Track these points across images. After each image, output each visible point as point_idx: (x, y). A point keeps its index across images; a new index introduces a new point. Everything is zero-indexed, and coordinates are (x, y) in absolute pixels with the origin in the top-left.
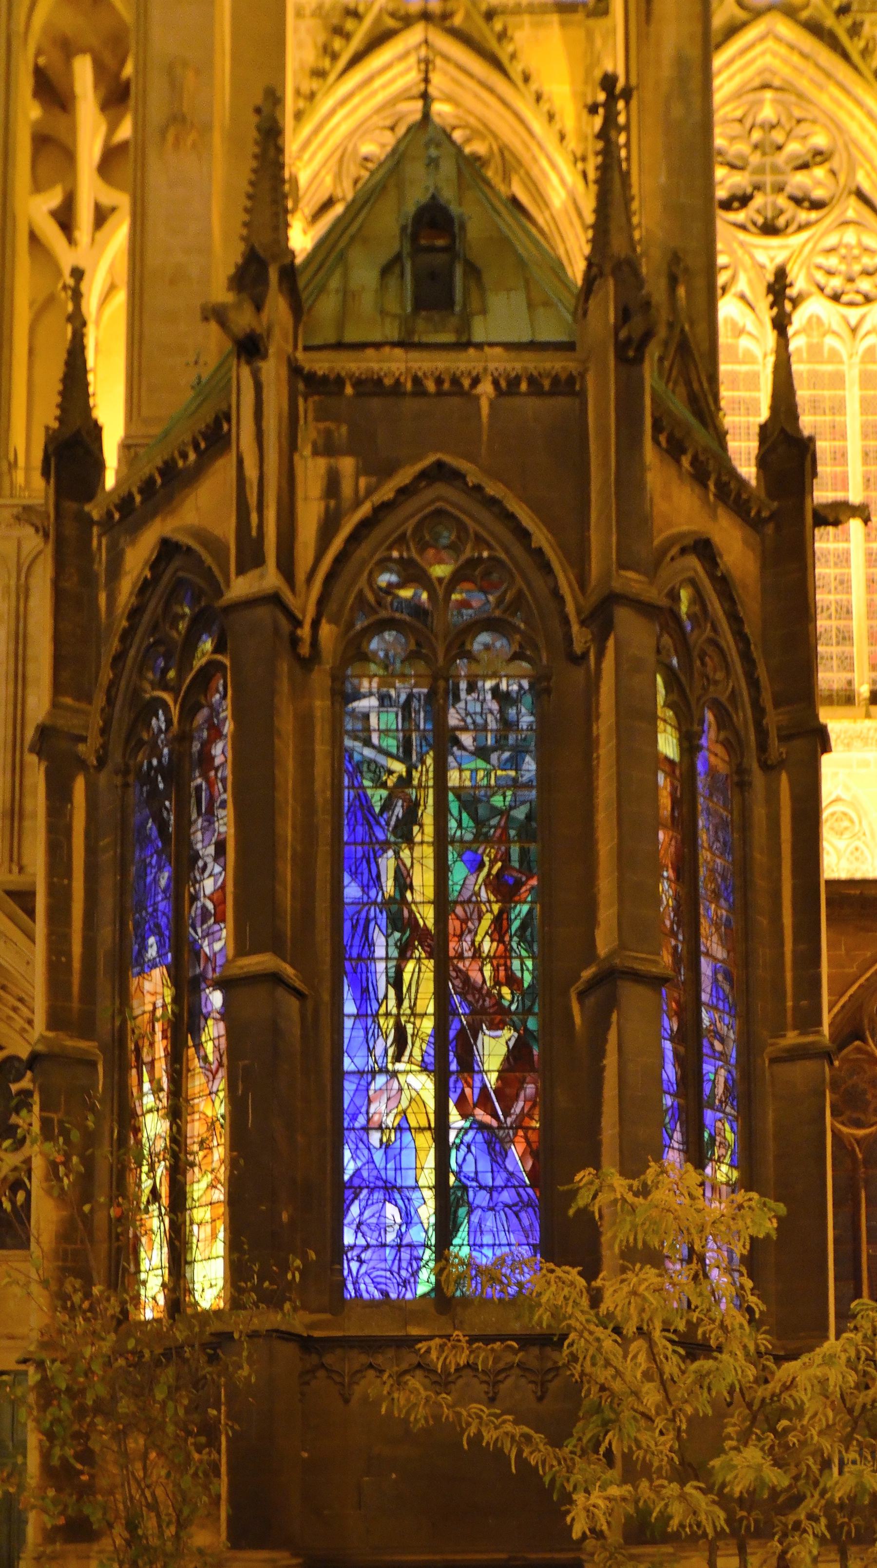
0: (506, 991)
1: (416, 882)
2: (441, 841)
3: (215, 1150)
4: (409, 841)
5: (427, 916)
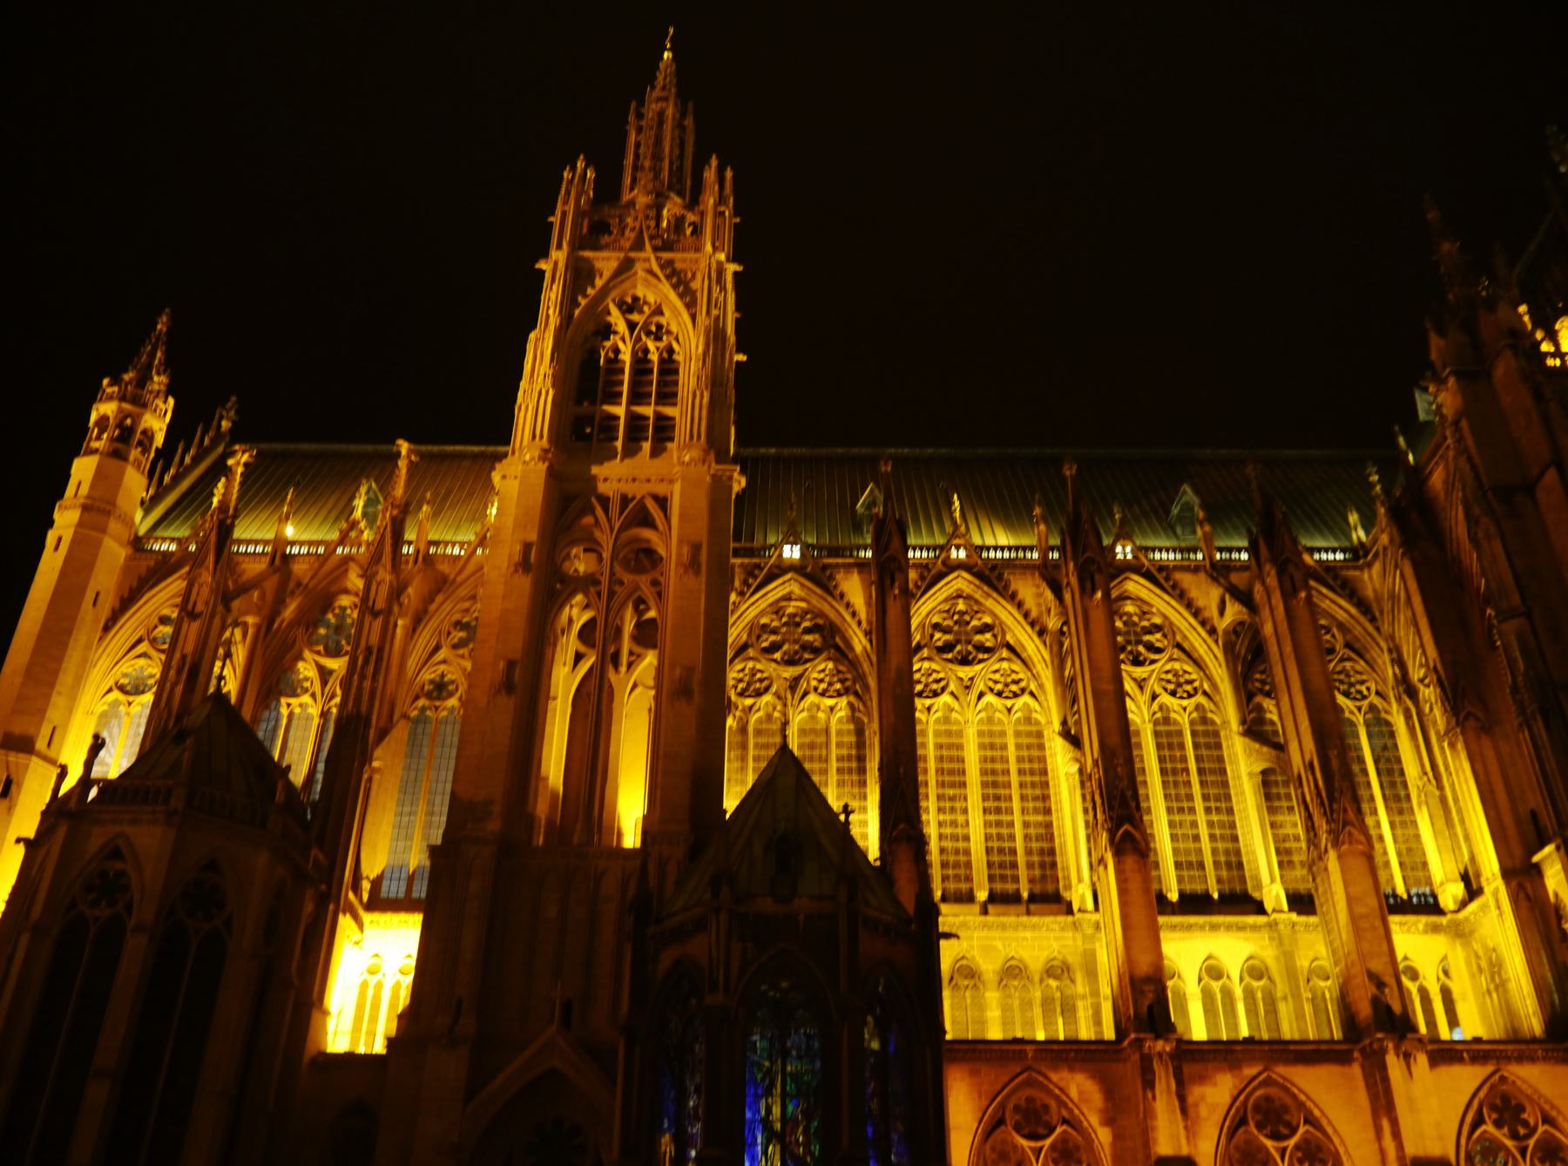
1: (774, 1111)
2: (784, 1096)
4: (772, 1095)
5: (778, 1126)
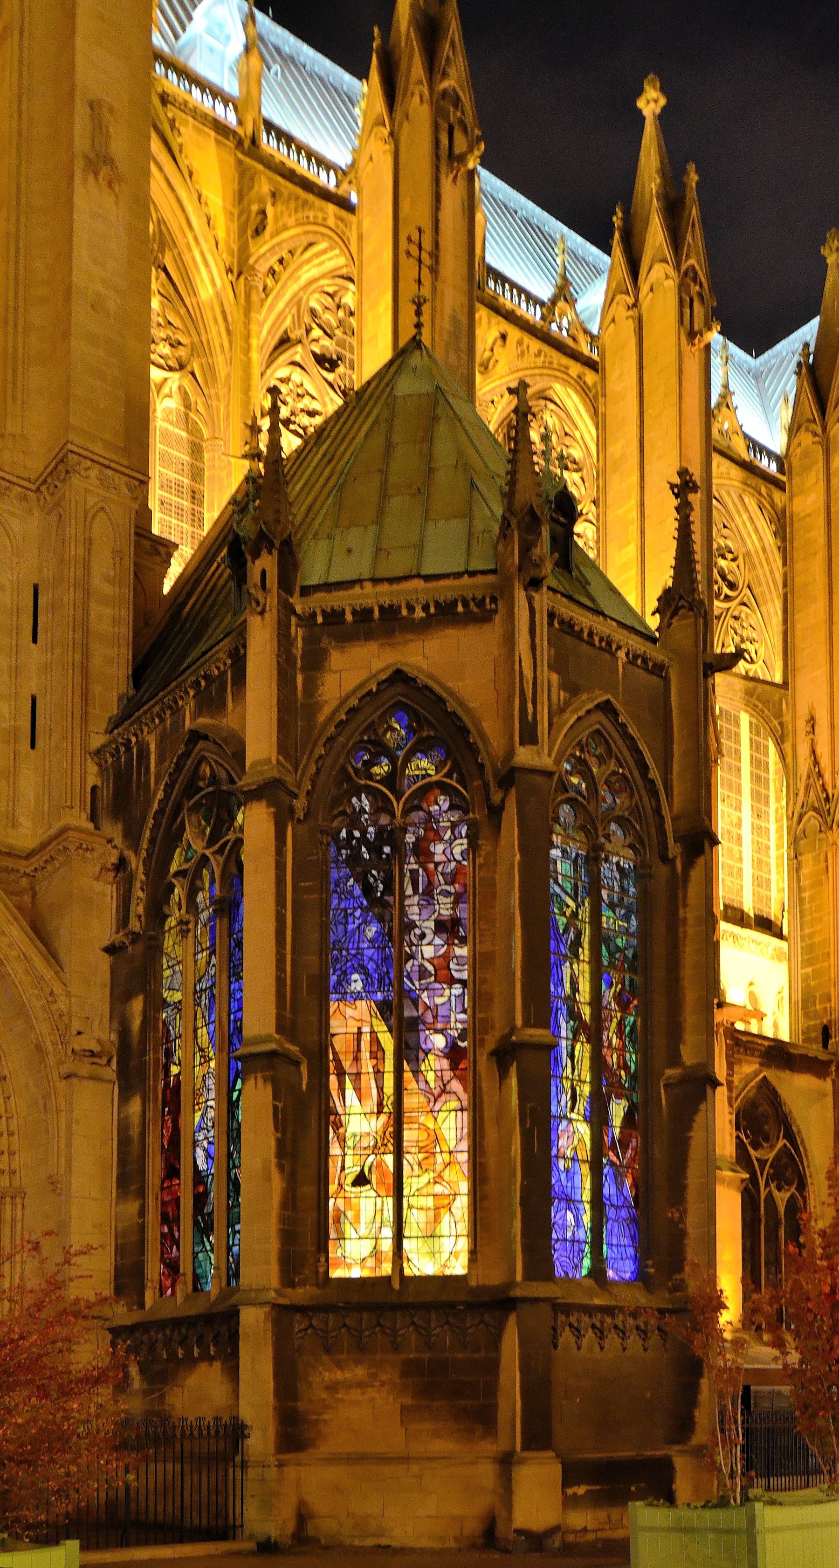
0: (623, 1073)
1: (581, 988)
3: (438, 1156)
5: (586, 1012)
